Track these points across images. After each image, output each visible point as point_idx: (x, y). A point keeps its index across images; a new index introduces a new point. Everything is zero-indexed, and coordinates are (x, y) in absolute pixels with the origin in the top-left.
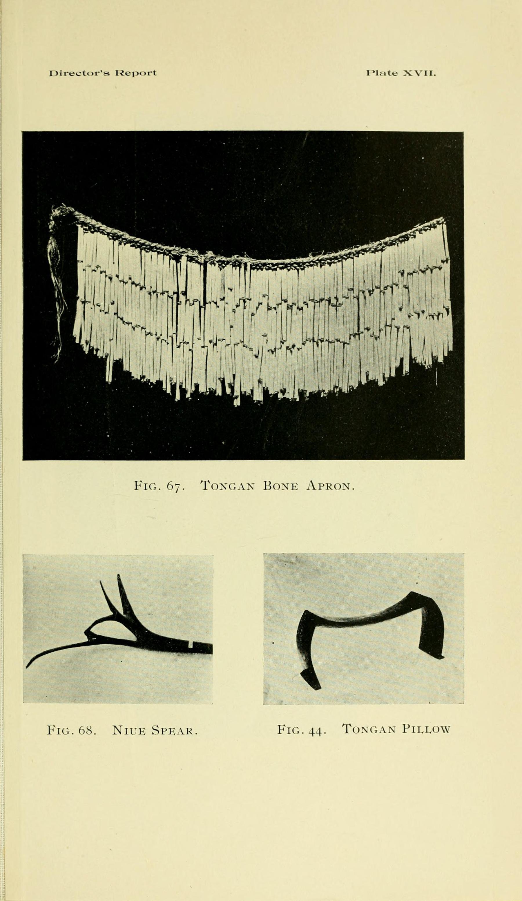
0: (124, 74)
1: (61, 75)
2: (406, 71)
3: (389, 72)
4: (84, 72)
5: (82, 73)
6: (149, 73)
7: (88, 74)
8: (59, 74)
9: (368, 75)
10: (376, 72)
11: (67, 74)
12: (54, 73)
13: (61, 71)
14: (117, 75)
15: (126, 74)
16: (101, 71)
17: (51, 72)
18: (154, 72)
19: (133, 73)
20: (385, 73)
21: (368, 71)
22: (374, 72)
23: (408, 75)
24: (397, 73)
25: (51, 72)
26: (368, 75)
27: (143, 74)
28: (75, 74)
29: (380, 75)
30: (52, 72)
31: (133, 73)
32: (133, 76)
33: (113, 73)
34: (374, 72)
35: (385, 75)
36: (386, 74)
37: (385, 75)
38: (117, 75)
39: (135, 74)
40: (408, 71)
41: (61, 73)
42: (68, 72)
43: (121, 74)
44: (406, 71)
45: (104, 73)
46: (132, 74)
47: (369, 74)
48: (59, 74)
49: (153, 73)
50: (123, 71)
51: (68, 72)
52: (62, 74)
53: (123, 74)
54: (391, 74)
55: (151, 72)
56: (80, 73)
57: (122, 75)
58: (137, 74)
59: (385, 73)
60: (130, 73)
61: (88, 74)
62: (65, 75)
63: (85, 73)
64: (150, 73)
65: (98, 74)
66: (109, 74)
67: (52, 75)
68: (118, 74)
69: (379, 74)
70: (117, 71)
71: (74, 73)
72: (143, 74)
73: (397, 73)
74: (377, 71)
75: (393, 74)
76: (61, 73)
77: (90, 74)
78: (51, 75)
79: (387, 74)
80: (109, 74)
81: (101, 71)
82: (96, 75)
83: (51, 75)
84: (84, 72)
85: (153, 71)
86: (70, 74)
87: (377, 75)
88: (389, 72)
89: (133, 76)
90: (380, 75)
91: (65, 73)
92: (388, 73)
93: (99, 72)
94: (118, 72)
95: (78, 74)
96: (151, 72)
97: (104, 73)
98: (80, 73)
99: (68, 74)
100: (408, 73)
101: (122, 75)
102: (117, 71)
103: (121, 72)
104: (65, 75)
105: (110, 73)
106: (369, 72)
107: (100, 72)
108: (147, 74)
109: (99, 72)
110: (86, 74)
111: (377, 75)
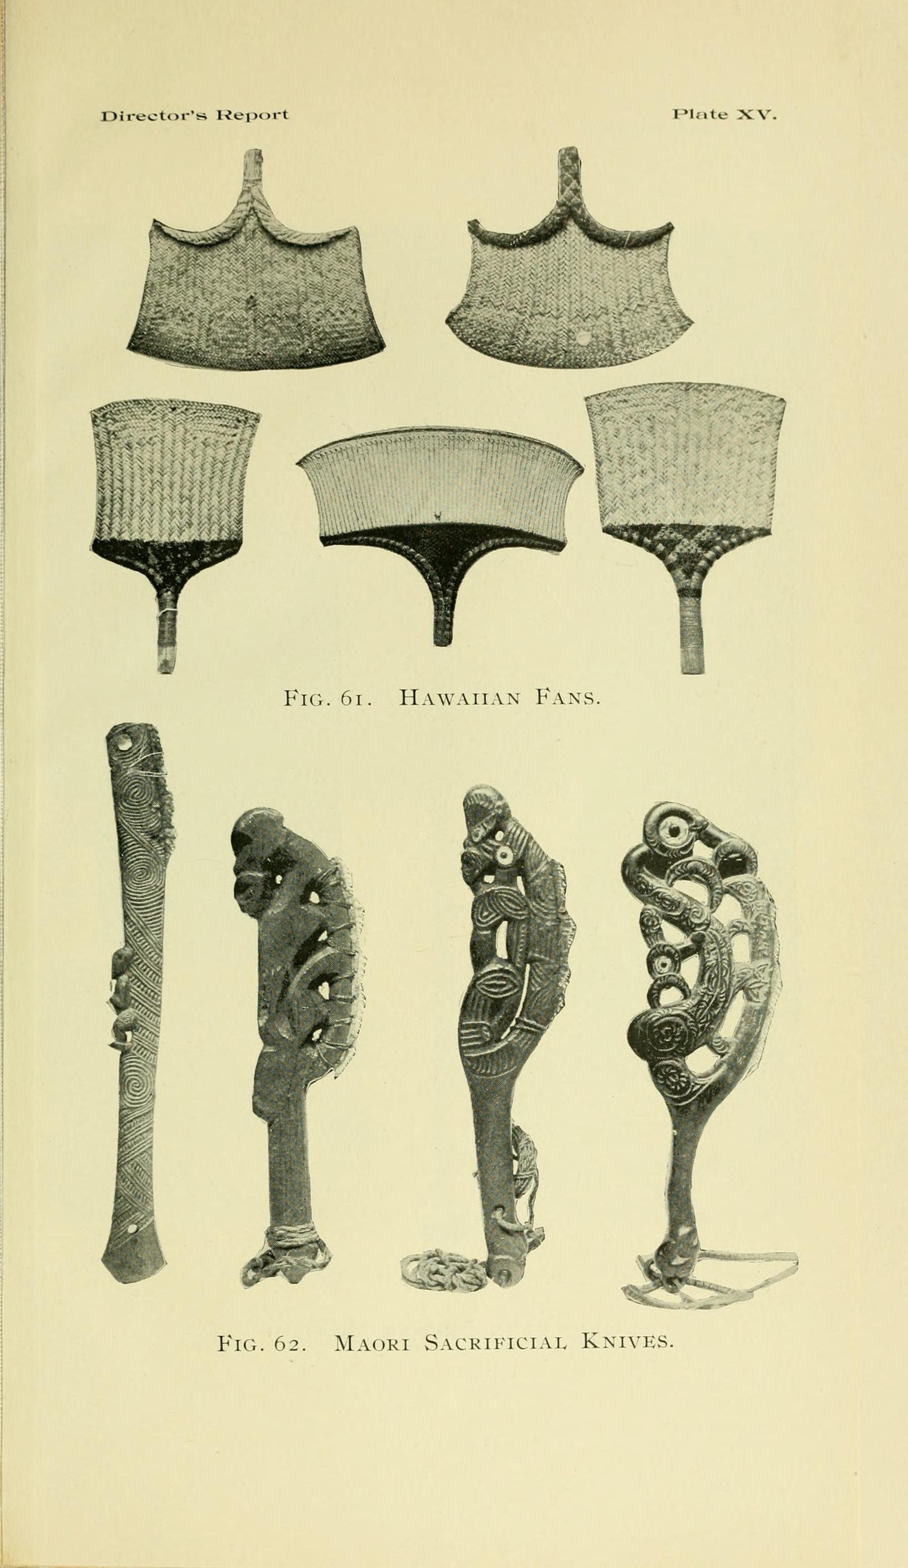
0: (232, 116)
1: (122, 119)
2: (742, 111)
3: (713, 113)
4: (162, 114)
5: (159, 116)
6: (275, 114)
7: (169, 117)
8: (119, 118)
9: (676, 117)
10: (689, 113)
11: (132, 117)
12: (110, 116)
13: (122, 112)
14: (220, 118)
15: (235, 116)
16: (193, 112)
17: (105, 114)
18: (285, 113)
19: (248, 115)
20: (705, 115)
21: (676, 111)
22: (686, 112)
23: (745, 117)
24: (726, 114)
25: (105, 114)
26: (676, 117)
27: (265, 116)
28: (147, 117)
29: (698, 117)
30: (107, 115)
31: (248, 115)
32: (248, 121)
33: (212, 115)
34: (686, 112)
35: (705, 117)
36: (707, 116)
37: (705, 117)
38: (220, 118)
39: (252, 116)
40: (746, 111)
41: (122, 117)
42: (134, 115)
43: (227, 116)
44: (742, 111)
45: (198, 115)
46: (246, 116)
47: (678, 116)
48: (119, 118)
49: (283, 114)
50: (230, 113)
51: (134, 115)
52: (124, 118)
53: (230, 116)
54: (716, 115)
55: (279, 113)
56: (156, 115)
57: (228, 118)
58: (254, 116)
59: (705, 115)
60: (242, 115)
61: (169, 117)
62: (129, 119)
63: (164, 115)
64: (277, 115)
65: (186, 116)
66: (205, 118)
67: (107, 119)
68: (222, 117)
69: (695, 115)
70: (220, 112)
71: (144, 116)
72: (265, 116)
73: (726, 114)
74: (692, 111)
75: (720, 115)
76: (122, 117)
77: (173, 117)
78: (105, 119)
79: (709, 115)
80: (205, 118)
81: (193, 112)
82: (183, 119)
83: (105, 119)
84: (162, 114)
85: (282, 111)
86: (138, 117)
87: (692, 117)
88: (713, 113)
89: (248, 121)
90: (698, 117)
91: (129, 116)
92: (710, 114)
93: (188, 114)
94: (222, 113)
95: (153, 117)
96: (279, 113)
97: (198, 115)
98: (156, 115)
99: (135, 117)
100: (746, 114)
101: (228, 118)
102: (220, 112)
103: (228, 113)
104: (129, 119)
105: (206, 116)
106: (679, 112)
107: (191, 113)
108: (272, 116)
109: (188, 114)
110: (165, 117)
111: (692, 117)
